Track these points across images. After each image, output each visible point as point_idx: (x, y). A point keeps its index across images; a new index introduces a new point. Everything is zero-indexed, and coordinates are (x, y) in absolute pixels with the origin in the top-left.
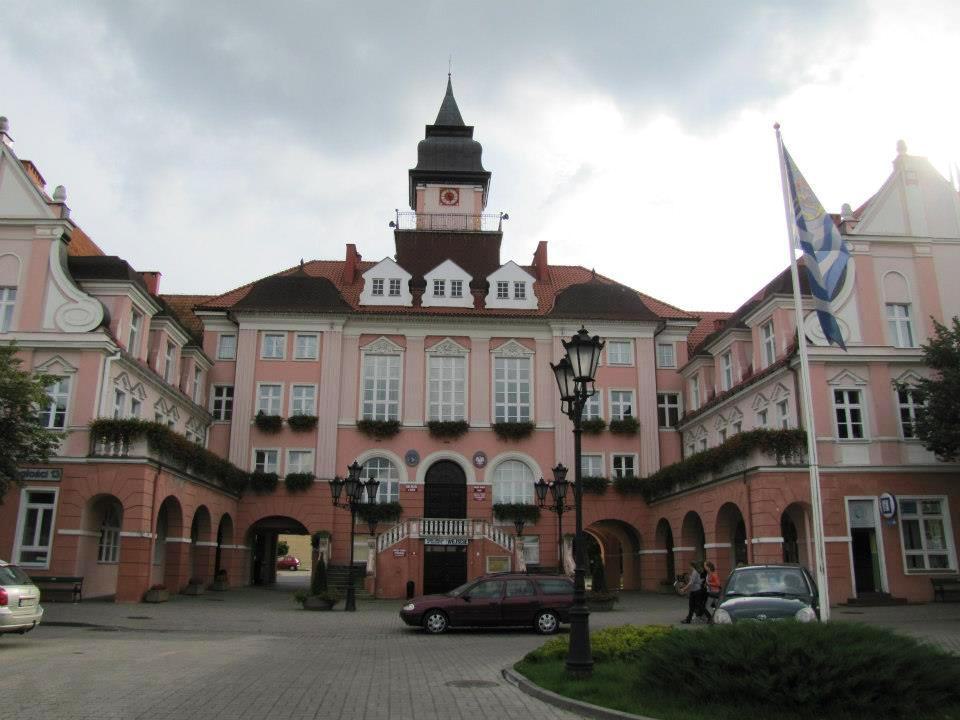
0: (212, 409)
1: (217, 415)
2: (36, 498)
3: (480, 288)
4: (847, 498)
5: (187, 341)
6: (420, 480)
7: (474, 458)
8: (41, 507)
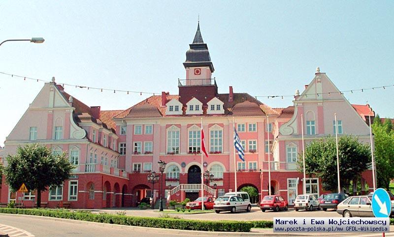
0: (119, 152)
1: (121, 153)
2: (72, 183)
3: (205, 108)
4: (288, 179)
6: (186, 171)
8: (74, 185)
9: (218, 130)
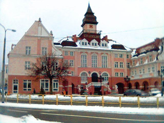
9: (105, 56)
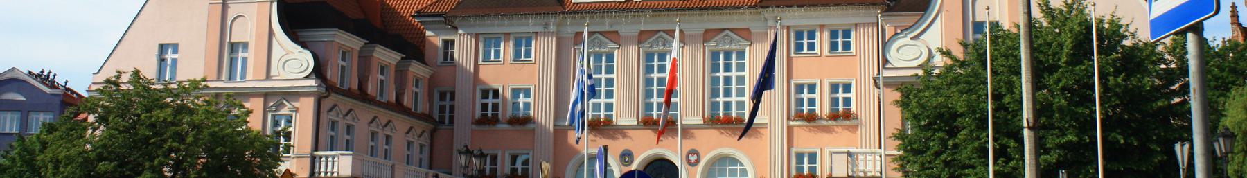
0: (436, 115)
1: (442, 122)
5: (399, 58)
7: (687, 156)
